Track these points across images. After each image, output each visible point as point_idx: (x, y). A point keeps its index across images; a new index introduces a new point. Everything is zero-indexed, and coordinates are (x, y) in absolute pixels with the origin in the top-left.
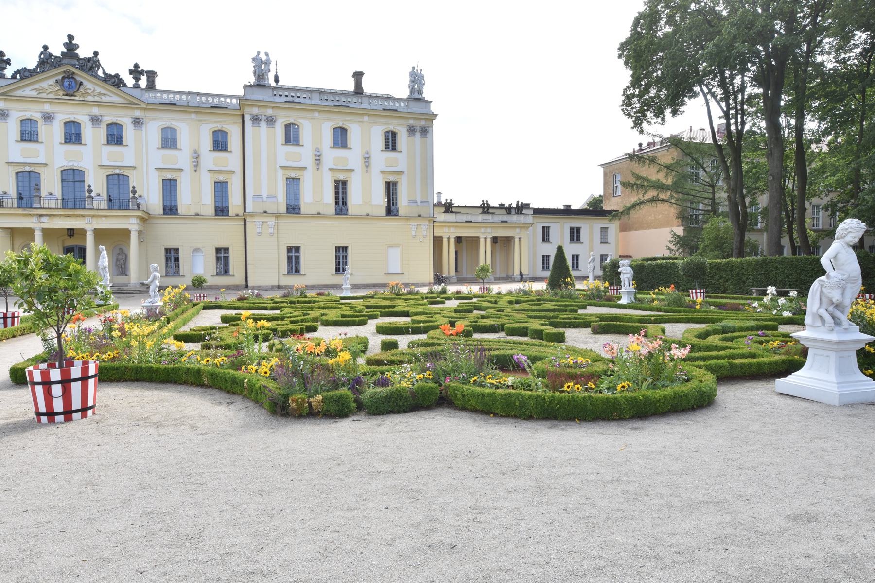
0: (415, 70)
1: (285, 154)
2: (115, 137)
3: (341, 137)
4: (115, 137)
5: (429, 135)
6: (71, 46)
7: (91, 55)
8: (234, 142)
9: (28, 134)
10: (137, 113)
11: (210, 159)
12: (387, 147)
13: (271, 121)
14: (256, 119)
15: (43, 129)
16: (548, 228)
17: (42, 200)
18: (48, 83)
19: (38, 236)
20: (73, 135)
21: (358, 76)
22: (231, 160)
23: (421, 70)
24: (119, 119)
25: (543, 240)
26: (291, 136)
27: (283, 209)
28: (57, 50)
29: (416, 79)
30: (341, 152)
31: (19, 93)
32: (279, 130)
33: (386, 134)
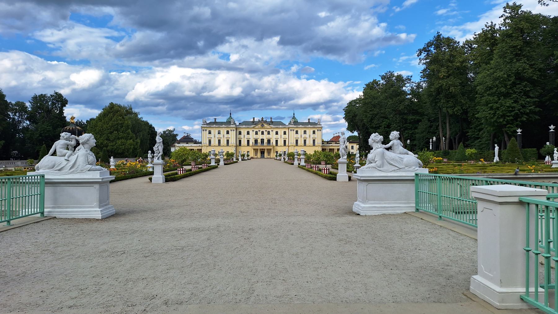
1: (296, 136)
2: (269, 133)
3: (305, 132)
4: (269, 133)
5: (321, 131)
8: (287, 133)
9: (256, 133)
10: (272, 129)
11: (283, 136)
12: (313, 133)
13: (293, 130)
14: (291, 130)
16: (353, 146)
18: (260, 126)
19: (259, 150)
20: (263, 133)
22: (287, 136)
25: (352, 149)
26: (297, 132)
27: (295, 145)
28: (260, 120)
30: (305, 135)
31: (255, 127)
32: (295, 131)
33: (313, 131)
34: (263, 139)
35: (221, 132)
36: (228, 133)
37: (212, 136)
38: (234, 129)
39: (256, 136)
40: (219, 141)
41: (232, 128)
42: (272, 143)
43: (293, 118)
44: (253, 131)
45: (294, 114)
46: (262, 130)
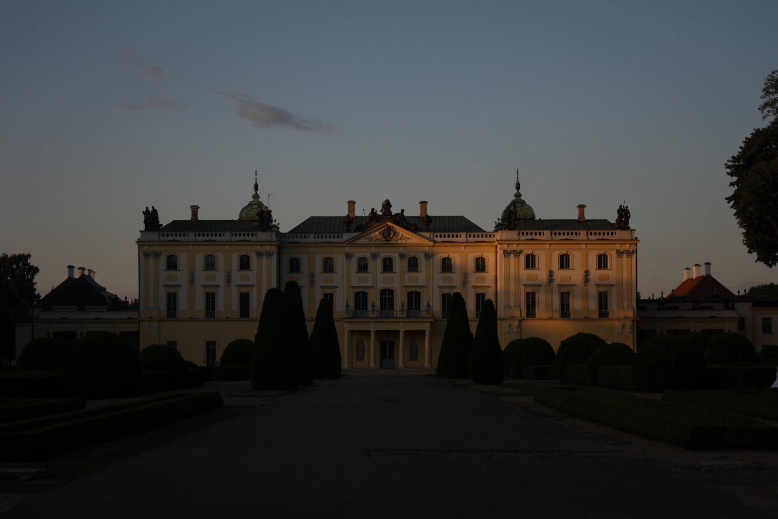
0: (622, 207)
6: (387, 205)
7: (400, 212)
9: (363, 267)
13: (517, 254)
15: (370, 263)
16: (770, 319)
17: (375, 313)
20: (388, 265)
21: (581, 207)
23: (627, 207)
24: (416, 254)
27: (524, 315)
29: (624, 214)
30: (565, 273)
33: (600, 257)
34: (391, 292)
35: (220, 263)
36: (245, 264)
37: (181, 276)
38: (268, 248)
39: (357, 280)
40: (210, 299)
41: (263, 243)
42: (429, 306)
43: (514, 203)
44: (349, 256)
45: (518, 187)
46: (385, 253)
